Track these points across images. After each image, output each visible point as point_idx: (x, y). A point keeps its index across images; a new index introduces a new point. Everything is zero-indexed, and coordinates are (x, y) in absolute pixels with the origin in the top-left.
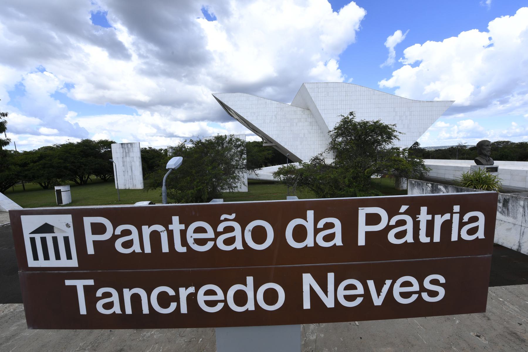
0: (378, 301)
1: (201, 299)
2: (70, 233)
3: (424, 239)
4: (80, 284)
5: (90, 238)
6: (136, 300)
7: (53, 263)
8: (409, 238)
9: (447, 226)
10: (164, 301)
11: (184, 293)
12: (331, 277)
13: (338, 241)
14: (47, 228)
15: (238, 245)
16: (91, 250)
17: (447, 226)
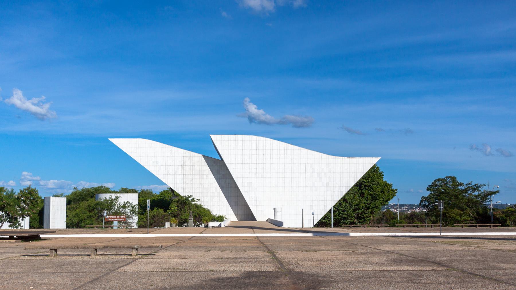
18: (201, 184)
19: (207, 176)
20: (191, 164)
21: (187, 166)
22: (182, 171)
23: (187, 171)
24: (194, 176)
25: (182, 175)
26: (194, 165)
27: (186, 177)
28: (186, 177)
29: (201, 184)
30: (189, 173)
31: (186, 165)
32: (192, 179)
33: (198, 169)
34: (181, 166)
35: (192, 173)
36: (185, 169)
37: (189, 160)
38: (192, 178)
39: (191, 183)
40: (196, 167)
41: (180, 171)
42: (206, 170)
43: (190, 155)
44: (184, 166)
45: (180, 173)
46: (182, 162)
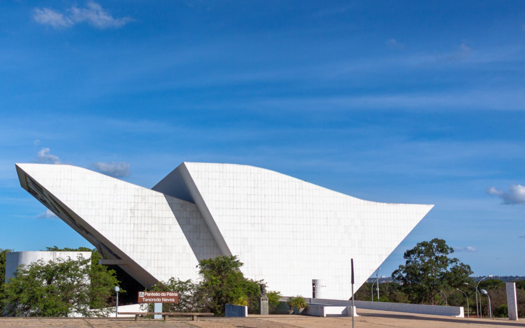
0: (169, 301)
1: (154, 300)
2: (144, 294)
3: (172, 295)
4: (144, 298)
5: (145, 294)
6: (148, 300)
7: (142, 296)
8: (171, 295)
9: (174, 295)
10: (151, 300)
11: (153, 299)
12: (165, 298)
13: (165, 295)
14: (142, 293)
15: (157, 295)
16: (145, 295)
17: (174, 295)
18: (161, 239)
19: (170, 228)
20: (147, 208)
21: (140, 211)
22: (132, 219)
23: (139, 219)
24: (150, 226)
25: (132, 225)
26: (151, 209)
27: (138, 229)
28: (138, 229)
29: (161, 239)
30: (143, 223)
31: (139, 209)
32: (148, 231)
33: (157, 216)
34: (131, 210)
35: (147, 223)
36: (136, 215)
37: (144, 201)
38: (147, 230)
39: (146, 238)
40: (153, 212)
41: (129, 219)
42: (169, 218)
43: (145, 194)
44: (136, 211)
45: (129, 222)
46: (133, 204)
